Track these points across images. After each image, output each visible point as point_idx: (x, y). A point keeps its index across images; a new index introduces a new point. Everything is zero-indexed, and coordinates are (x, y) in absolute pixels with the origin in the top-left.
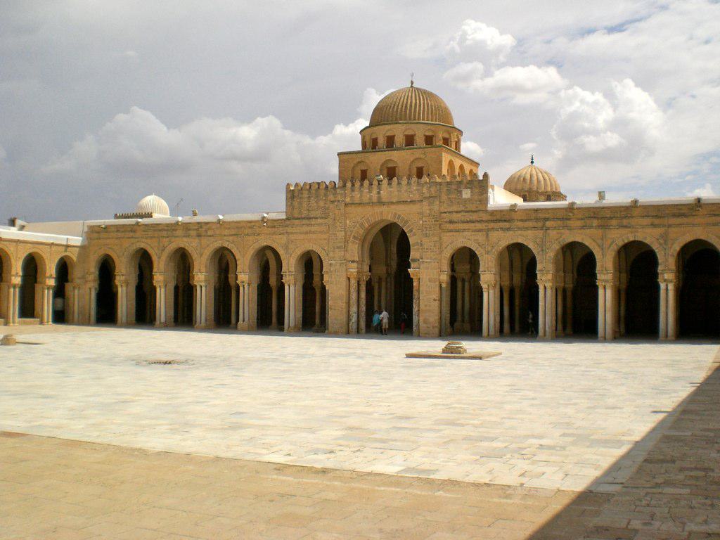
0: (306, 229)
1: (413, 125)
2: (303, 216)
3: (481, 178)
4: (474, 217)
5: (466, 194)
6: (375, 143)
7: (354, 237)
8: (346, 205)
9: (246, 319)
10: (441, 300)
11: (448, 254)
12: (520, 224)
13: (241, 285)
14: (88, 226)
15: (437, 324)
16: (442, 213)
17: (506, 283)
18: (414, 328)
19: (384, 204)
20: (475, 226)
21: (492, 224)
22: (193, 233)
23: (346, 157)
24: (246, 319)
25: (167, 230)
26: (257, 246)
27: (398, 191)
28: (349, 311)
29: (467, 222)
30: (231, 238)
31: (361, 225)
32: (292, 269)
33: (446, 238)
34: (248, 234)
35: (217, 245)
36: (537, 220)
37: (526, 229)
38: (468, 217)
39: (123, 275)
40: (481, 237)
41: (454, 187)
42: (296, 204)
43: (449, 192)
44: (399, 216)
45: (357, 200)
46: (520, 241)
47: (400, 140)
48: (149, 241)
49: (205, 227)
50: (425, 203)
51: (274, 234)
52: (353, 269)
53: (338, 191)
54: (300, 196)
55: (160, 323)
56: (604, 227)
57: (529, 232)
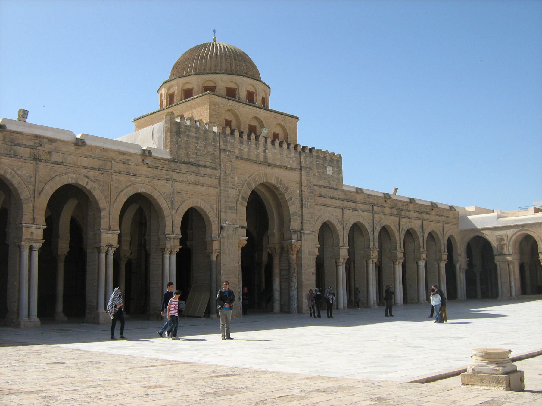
0: (192, 178)
4: (335, 194)
5: (330, 171)
16: (315, 185)
19: (269, 165)
26: (131, 191)
27: (280, 154)
29: (331, 198)
30: (92, 174)
31: (249, 185)
35: (68, 179)
42: (182, 141)
44: (281, 181)
46: (361, 220)
50: (303, 172)
51: (155, 177)
54: (187, 133)
56: (399, 216)
57: (366, 213)
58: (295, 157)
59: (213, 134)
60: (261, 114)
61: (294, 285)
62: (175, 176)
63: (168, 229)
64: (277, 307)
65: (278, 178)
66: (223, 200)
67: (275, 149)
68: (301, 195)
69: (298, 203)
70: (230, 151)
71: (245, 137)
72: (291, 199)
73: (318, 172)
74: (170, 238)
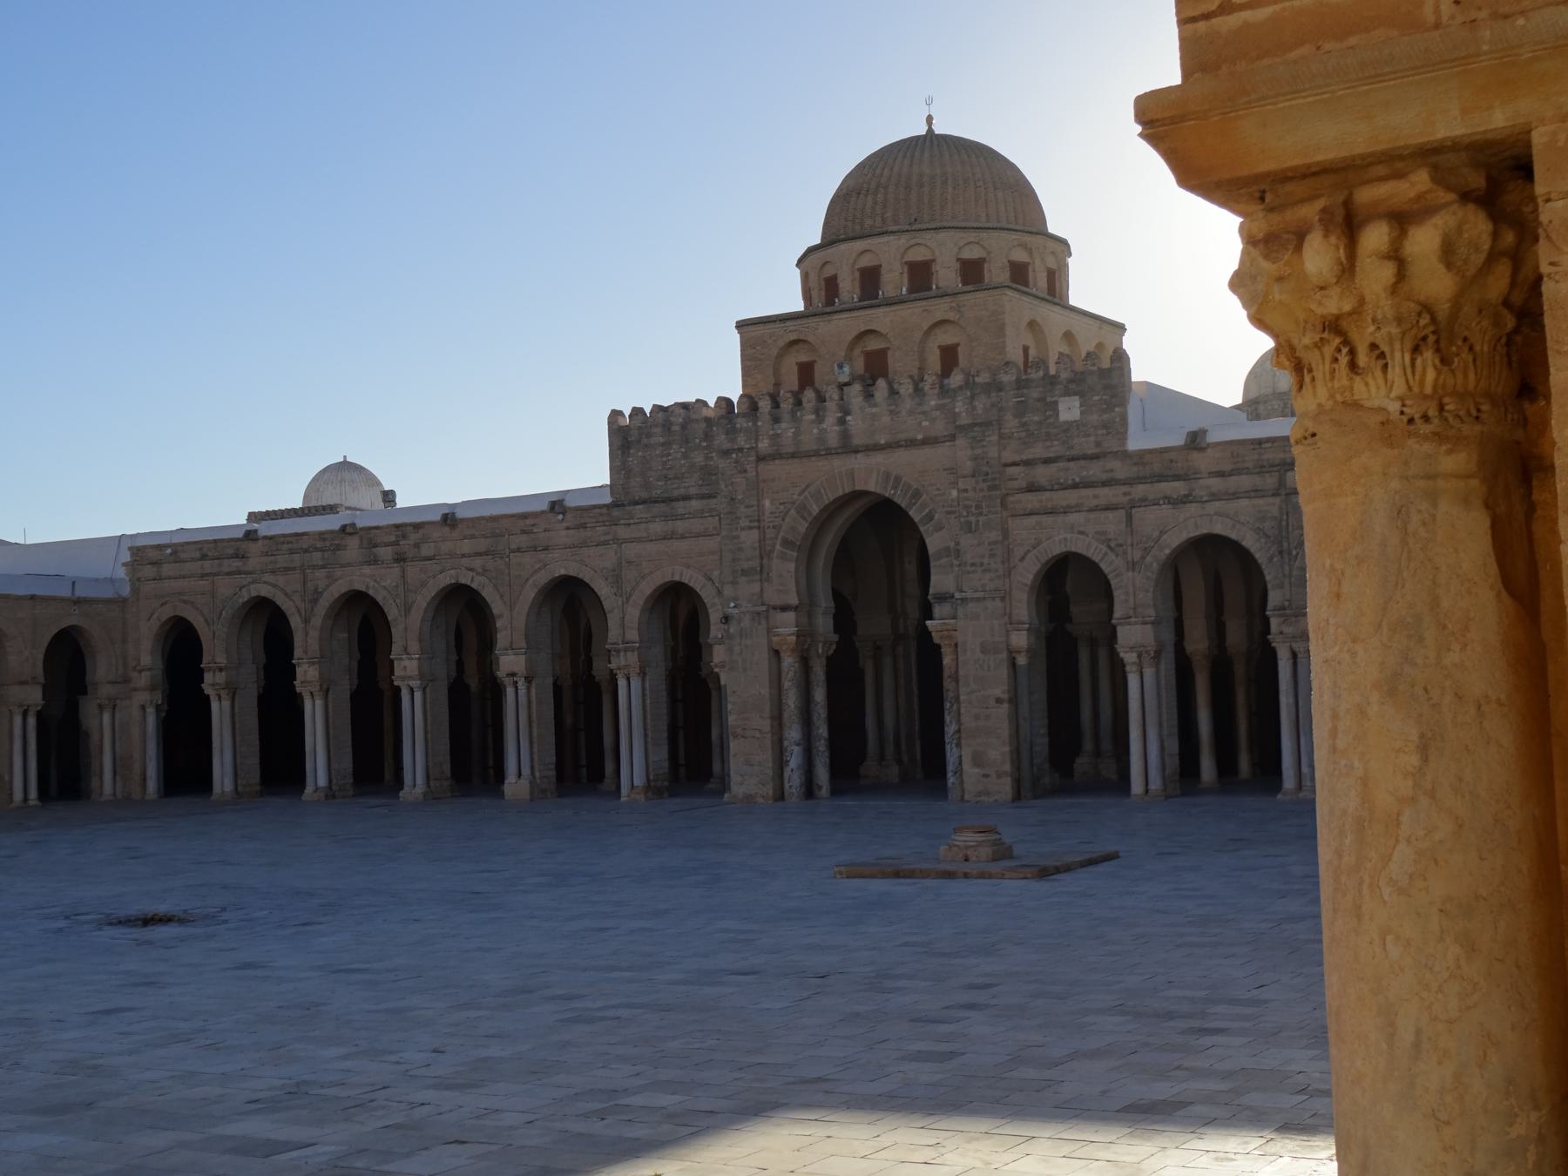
0: (657, 527)
1: (928, 235)
2: (656, 493)
3: (1106, 364)
4: (1095, 470)
5: (1069, 409)
6: (831, 286)
7: (786, 543)
8: (761, 459)
9: (526, 771)
10: (1014, 701)
11: (1028, 572)
12: (1216, 483)
13: (507, 681)
14: (130, 549)
15: (1007, 767)
16: (1006, 465)
17: (1198, 642)
18: (951, 779)
19: (857, 452)
20: (1096, 497)
21: (1141, 488)
22: (385, 553)
23: (760, 330)
24: (526, 771)
25: (322, 550)
26: (543, 578)
27: (891, 412)
28: (781, 741)
29: (1075, 486)
30: (478, 563)
32: (633, 635)
33: (1022, 530)
34: (519, 550)
35: (446, 579)
36: (1261, 469)
37: (1235, 496)
38: (1076, 472)
39: (221, 670)
40: (1112, 523)
41: (1035, 394)
43: (1021, 410)
44: (898, 479)
45: (789, 448)
46: (1219, 529)
47: (894, 281)
48: (280, 580)
49: (414, 537)
50: (960, 442)
51: (584, 544)
52: (787, 626)
53: (741, 423)
54: (645, 441)
55: (317, 789)
57: (1244, 502)
58: (938, 408)
59: (703, 425)
62: (622, 532)
65: (887, 475)
67: (875, 405)
70: (741, 450)
72: (930, 517)
73: (1024, 424)
74: (618, 651)
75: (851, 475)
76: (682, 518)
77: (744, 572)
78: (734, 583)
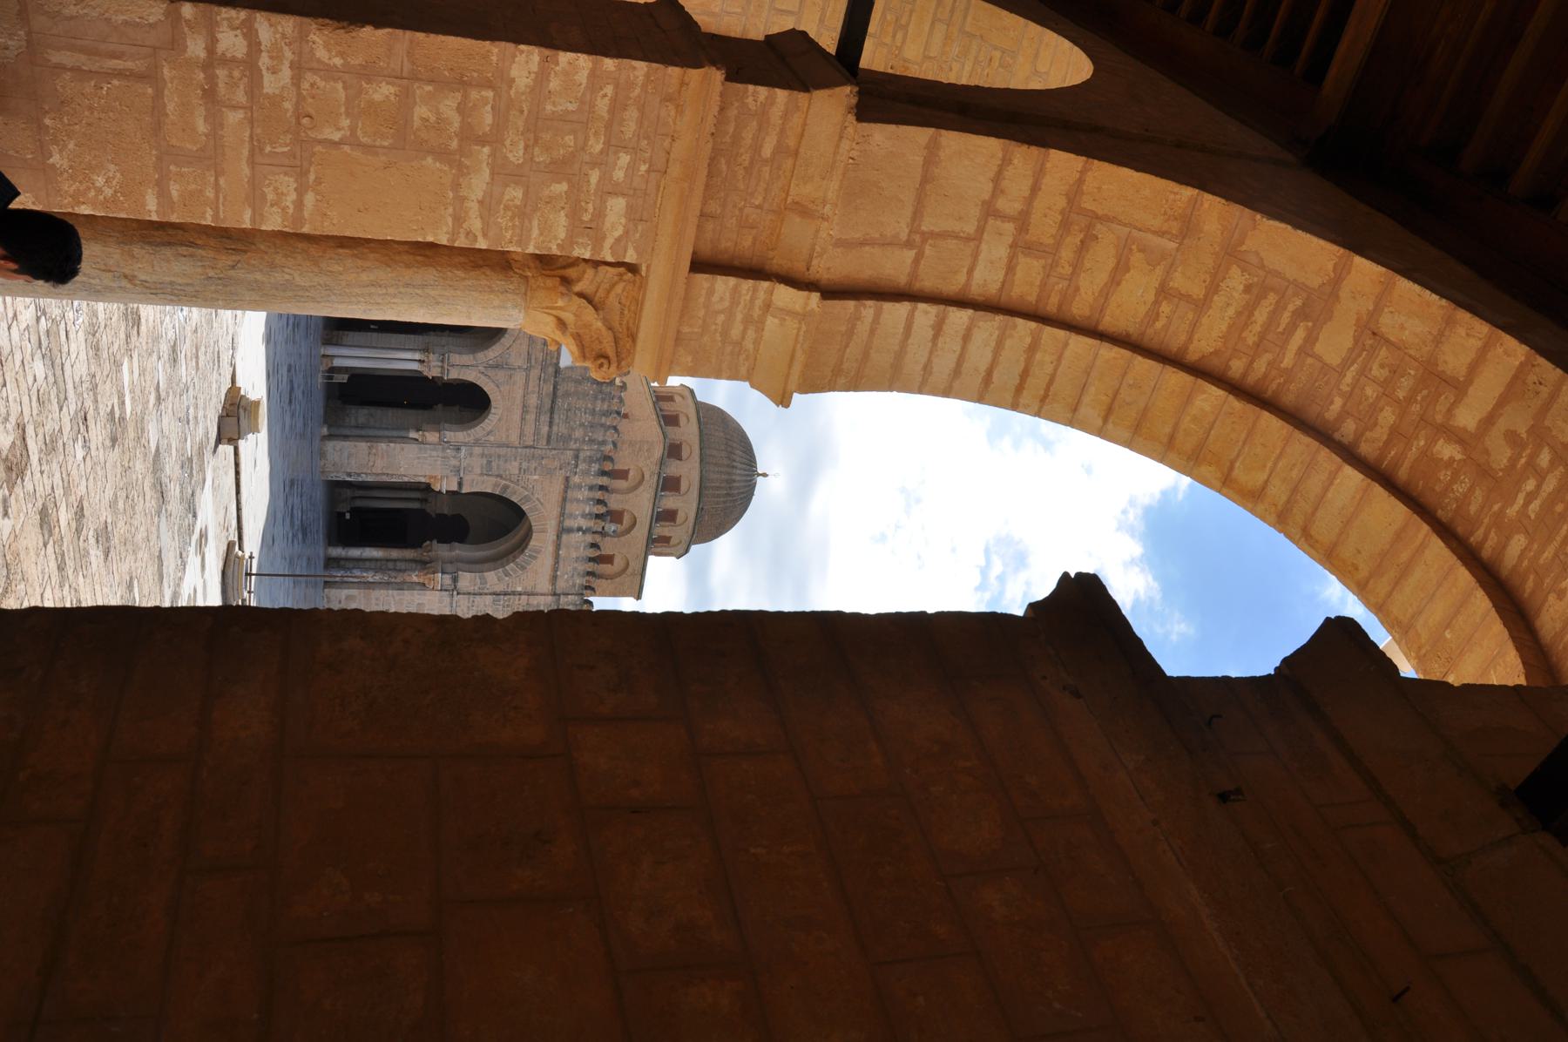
0: (533, 400)
8: (567, 479)
19: (559, 537)
31: (527, 499)
32: (454, 374)
60: (641, 532)
61: (370, 577)
63: (456, 358)
64: (337, 552)
65: (538, 552)
66: (502, 451)
68: (514, 593)
69: (499, 588)
71: (599, 495)
75: (544, 531)
76: (537, 420)
77: (489, 463)
78: (483, 455)
